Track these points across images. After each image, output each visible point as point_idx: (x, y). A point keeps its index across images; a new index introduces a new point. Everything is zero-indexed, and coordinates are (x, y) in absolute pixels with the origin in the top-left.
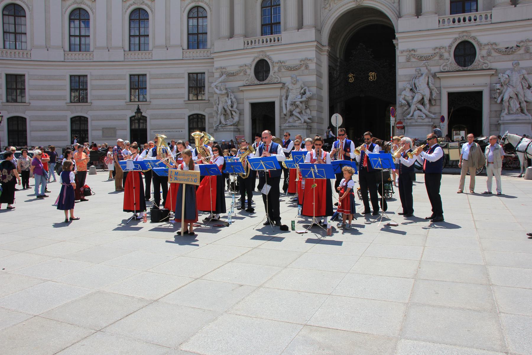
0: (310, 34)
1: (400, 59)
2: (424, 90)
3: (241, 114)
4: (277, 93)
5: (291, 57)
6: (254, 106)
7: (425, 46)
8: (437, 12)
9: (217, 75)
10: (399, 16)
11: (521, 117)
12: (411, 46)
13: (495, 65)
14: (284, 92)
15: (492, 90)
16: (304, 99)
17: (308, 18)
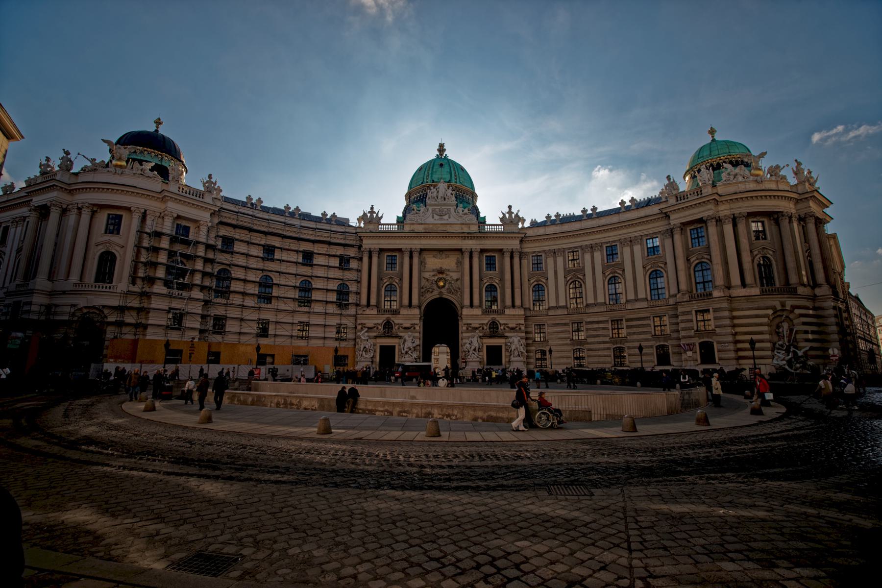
0: (417, 311)
1: (462, 328)
2: (476, 344)
3: (375, 351)
4: (397, 340)
5: (407, 324)
6: (381, 347)
7: (475, 323)
8: (480, 306)
9: (359, 327)
10: (462, 308)
11: (518, 358)
12: (469, 322)
13: (507, 334)
14: (402, 341)
15: (506, 345)
16: (414, 345)
17: (415, 301)
